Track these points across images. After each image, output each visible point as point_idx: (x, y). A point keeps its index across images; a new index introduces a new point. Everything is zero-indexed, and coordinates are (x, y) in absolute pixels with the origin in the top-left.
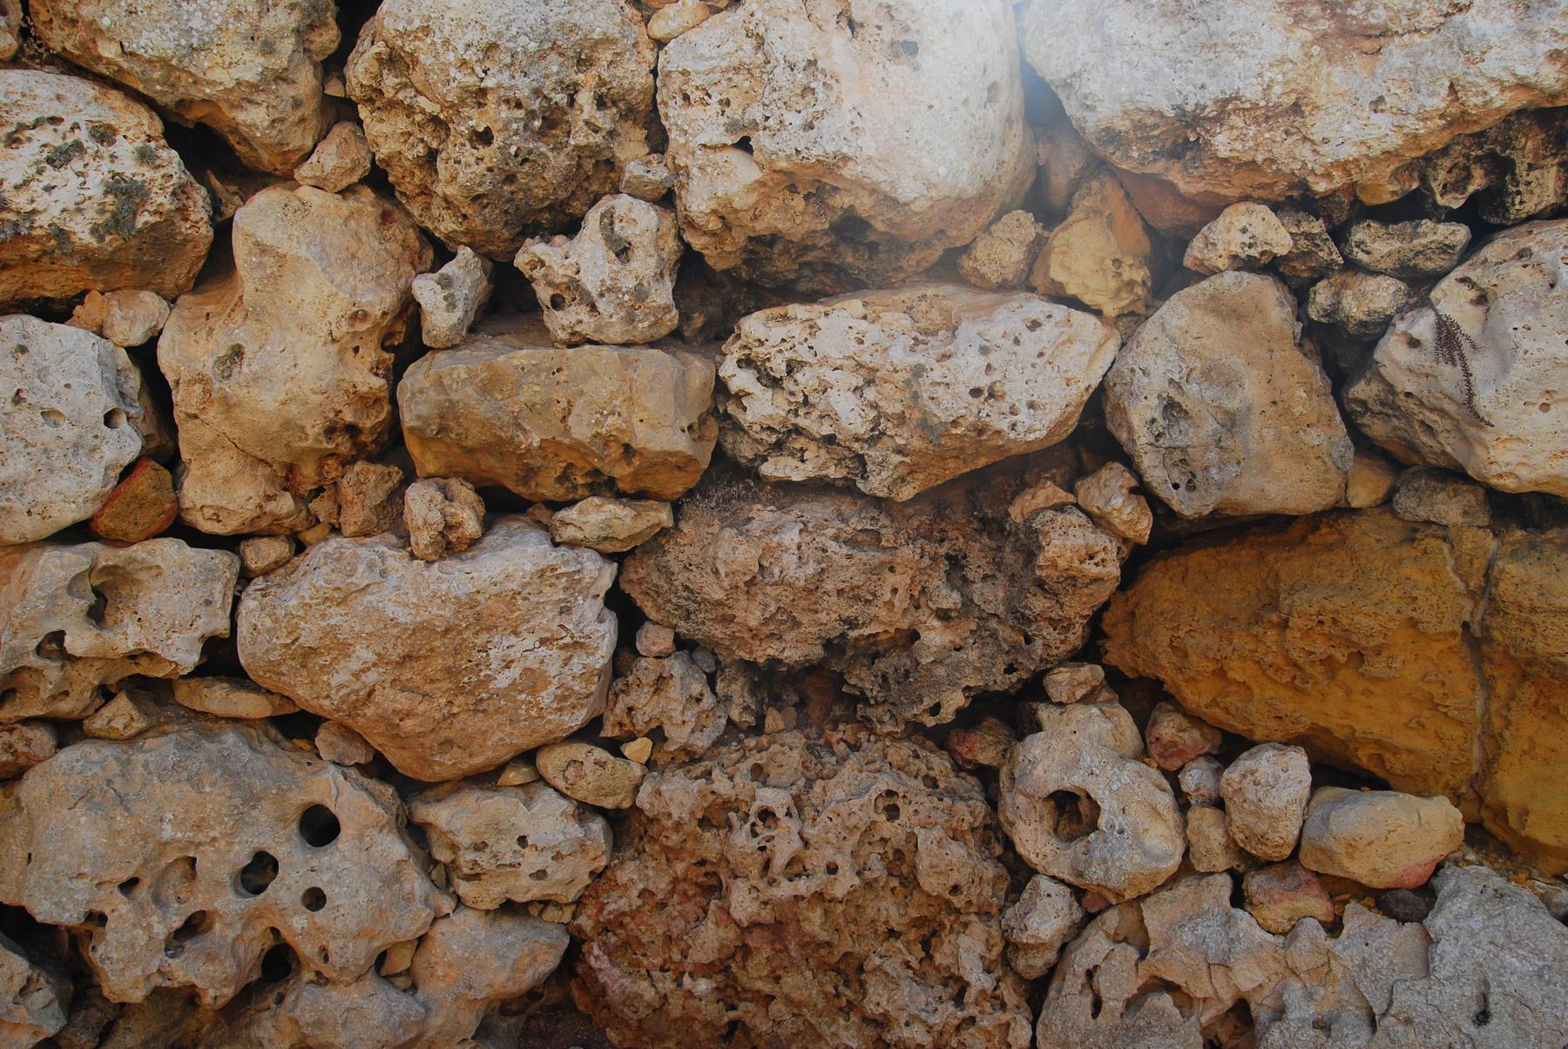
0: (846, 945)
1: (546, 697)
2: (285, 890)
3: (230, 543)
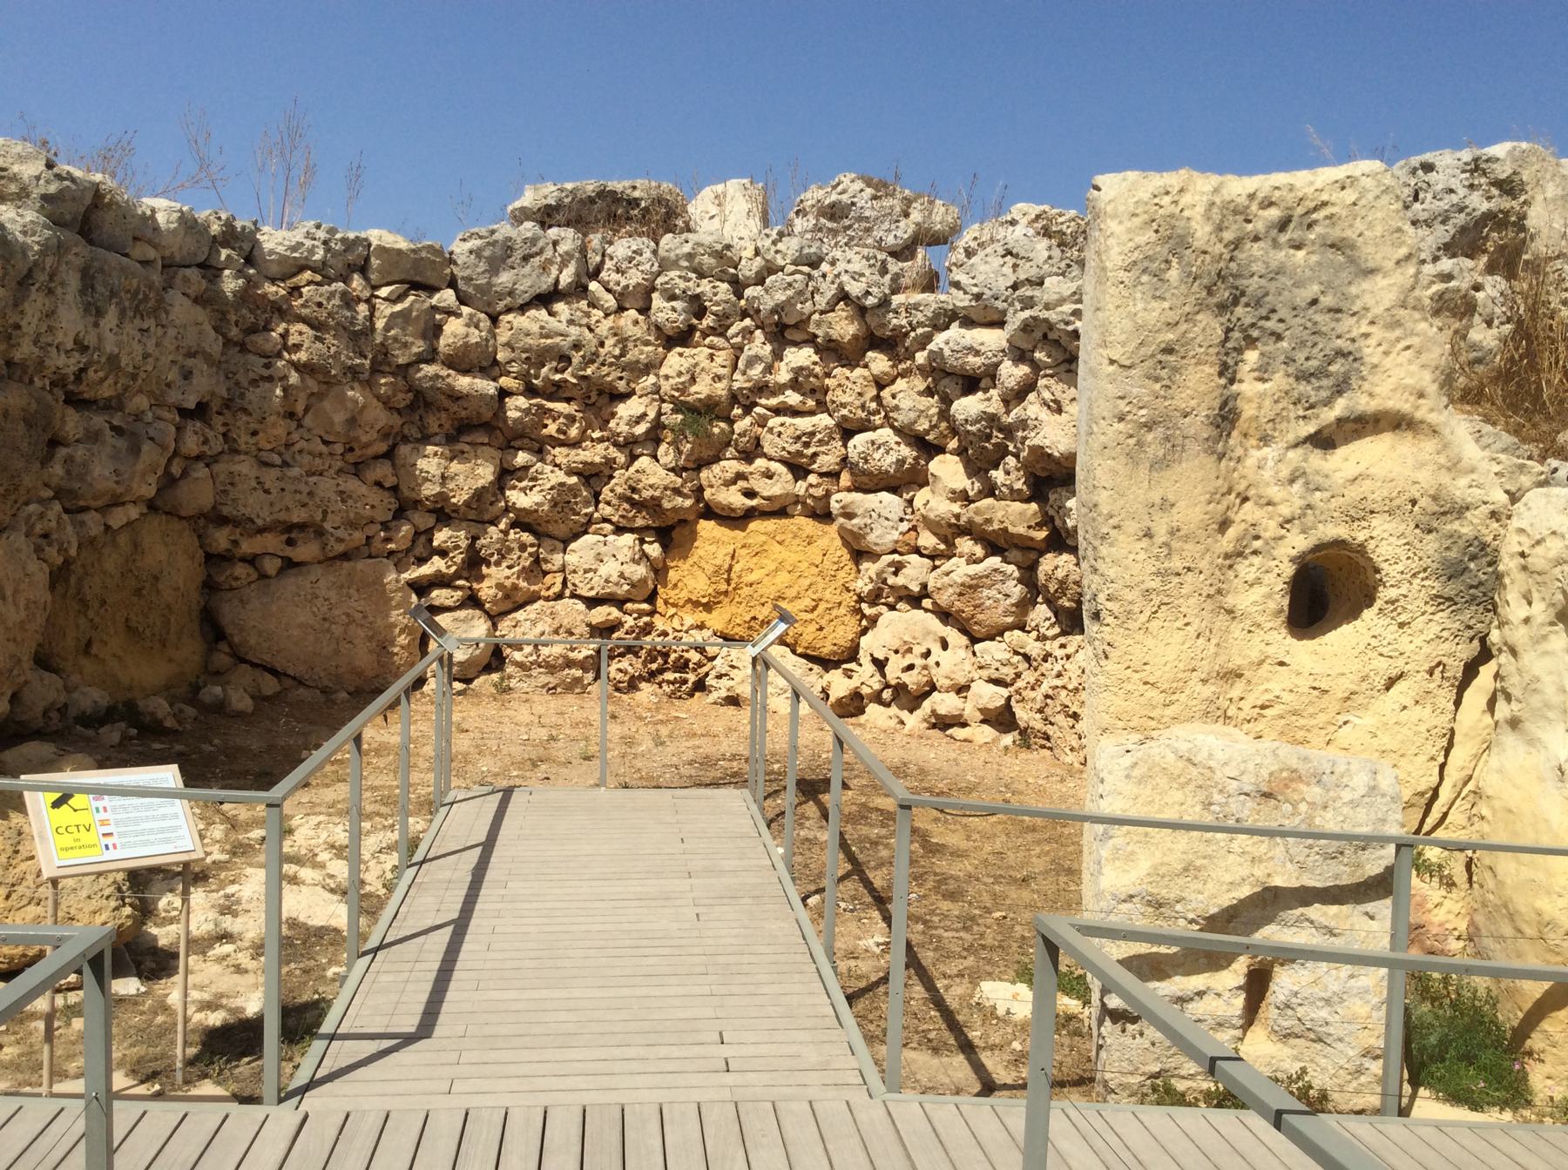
0: (1074, 709)
1: (1000, 610)
2: (931, 661)
3: (932, 557)
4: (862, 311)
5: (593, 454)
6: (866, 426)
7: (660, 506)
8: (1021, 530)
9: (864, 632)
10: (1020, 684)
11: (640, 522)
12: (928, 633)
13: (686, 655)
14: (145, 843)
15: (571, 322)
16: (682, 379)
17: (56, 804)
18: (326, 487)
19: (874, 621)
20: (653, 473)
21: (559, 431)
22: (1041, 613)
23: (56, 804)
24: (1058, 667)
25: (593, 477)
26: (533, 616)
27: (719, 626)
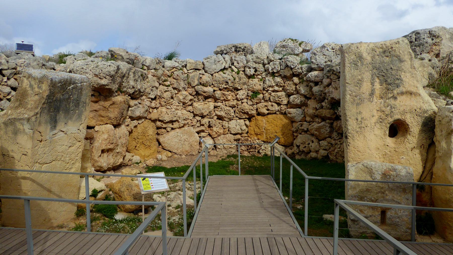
2: (310, 145)
3: (309, 122)
6: (293, 94)
8: (329, 116)
9: (294, 139)
10: (330, 150)
11: (244, 117)
12: (309, 139)
14: (159, 187)
17: (143, 180)
18: (179, 113)
19: (297, 136)
20: (247, 106)
22: (335, 135)
23: (143, 180)
24: (339, 146)
27: (262, 139)
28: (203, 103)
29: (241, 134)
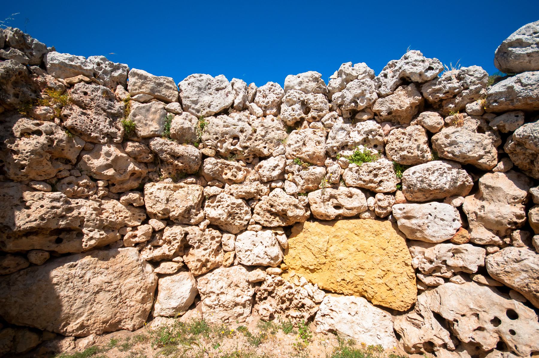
4: (419, 86)
5: (250, 188)
7: (286, 215)
11: (275, 224)
12: (494, 304)
13: (303, 301)
15: (240, 120)
16: (298, 145)
20: (282, 197)
21: (232, 175)
25: (249, 199)
26: (216, 278)
27: (321, 284)
28: (172, 185)
29: (264, 268)
